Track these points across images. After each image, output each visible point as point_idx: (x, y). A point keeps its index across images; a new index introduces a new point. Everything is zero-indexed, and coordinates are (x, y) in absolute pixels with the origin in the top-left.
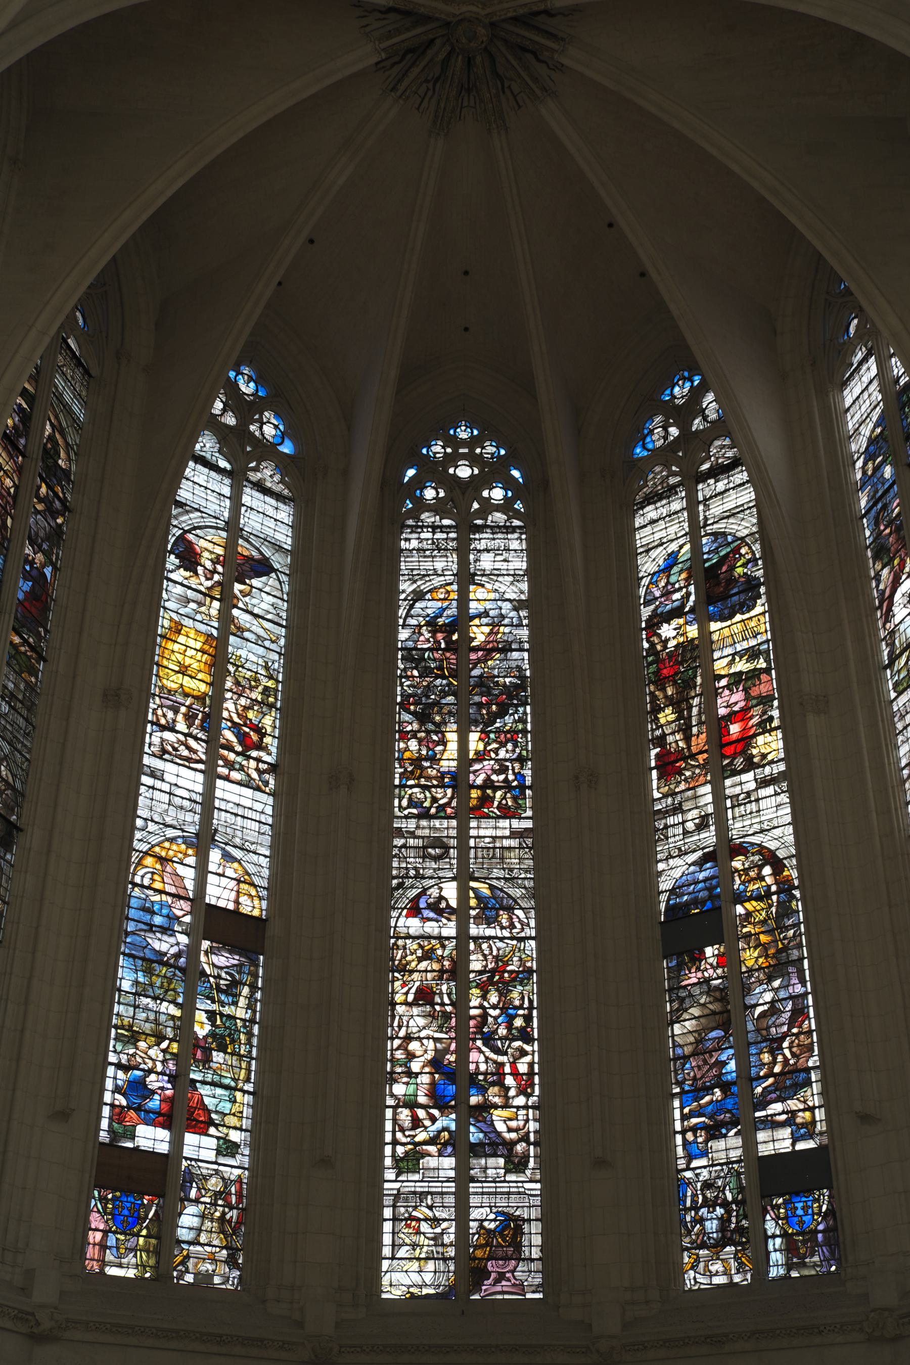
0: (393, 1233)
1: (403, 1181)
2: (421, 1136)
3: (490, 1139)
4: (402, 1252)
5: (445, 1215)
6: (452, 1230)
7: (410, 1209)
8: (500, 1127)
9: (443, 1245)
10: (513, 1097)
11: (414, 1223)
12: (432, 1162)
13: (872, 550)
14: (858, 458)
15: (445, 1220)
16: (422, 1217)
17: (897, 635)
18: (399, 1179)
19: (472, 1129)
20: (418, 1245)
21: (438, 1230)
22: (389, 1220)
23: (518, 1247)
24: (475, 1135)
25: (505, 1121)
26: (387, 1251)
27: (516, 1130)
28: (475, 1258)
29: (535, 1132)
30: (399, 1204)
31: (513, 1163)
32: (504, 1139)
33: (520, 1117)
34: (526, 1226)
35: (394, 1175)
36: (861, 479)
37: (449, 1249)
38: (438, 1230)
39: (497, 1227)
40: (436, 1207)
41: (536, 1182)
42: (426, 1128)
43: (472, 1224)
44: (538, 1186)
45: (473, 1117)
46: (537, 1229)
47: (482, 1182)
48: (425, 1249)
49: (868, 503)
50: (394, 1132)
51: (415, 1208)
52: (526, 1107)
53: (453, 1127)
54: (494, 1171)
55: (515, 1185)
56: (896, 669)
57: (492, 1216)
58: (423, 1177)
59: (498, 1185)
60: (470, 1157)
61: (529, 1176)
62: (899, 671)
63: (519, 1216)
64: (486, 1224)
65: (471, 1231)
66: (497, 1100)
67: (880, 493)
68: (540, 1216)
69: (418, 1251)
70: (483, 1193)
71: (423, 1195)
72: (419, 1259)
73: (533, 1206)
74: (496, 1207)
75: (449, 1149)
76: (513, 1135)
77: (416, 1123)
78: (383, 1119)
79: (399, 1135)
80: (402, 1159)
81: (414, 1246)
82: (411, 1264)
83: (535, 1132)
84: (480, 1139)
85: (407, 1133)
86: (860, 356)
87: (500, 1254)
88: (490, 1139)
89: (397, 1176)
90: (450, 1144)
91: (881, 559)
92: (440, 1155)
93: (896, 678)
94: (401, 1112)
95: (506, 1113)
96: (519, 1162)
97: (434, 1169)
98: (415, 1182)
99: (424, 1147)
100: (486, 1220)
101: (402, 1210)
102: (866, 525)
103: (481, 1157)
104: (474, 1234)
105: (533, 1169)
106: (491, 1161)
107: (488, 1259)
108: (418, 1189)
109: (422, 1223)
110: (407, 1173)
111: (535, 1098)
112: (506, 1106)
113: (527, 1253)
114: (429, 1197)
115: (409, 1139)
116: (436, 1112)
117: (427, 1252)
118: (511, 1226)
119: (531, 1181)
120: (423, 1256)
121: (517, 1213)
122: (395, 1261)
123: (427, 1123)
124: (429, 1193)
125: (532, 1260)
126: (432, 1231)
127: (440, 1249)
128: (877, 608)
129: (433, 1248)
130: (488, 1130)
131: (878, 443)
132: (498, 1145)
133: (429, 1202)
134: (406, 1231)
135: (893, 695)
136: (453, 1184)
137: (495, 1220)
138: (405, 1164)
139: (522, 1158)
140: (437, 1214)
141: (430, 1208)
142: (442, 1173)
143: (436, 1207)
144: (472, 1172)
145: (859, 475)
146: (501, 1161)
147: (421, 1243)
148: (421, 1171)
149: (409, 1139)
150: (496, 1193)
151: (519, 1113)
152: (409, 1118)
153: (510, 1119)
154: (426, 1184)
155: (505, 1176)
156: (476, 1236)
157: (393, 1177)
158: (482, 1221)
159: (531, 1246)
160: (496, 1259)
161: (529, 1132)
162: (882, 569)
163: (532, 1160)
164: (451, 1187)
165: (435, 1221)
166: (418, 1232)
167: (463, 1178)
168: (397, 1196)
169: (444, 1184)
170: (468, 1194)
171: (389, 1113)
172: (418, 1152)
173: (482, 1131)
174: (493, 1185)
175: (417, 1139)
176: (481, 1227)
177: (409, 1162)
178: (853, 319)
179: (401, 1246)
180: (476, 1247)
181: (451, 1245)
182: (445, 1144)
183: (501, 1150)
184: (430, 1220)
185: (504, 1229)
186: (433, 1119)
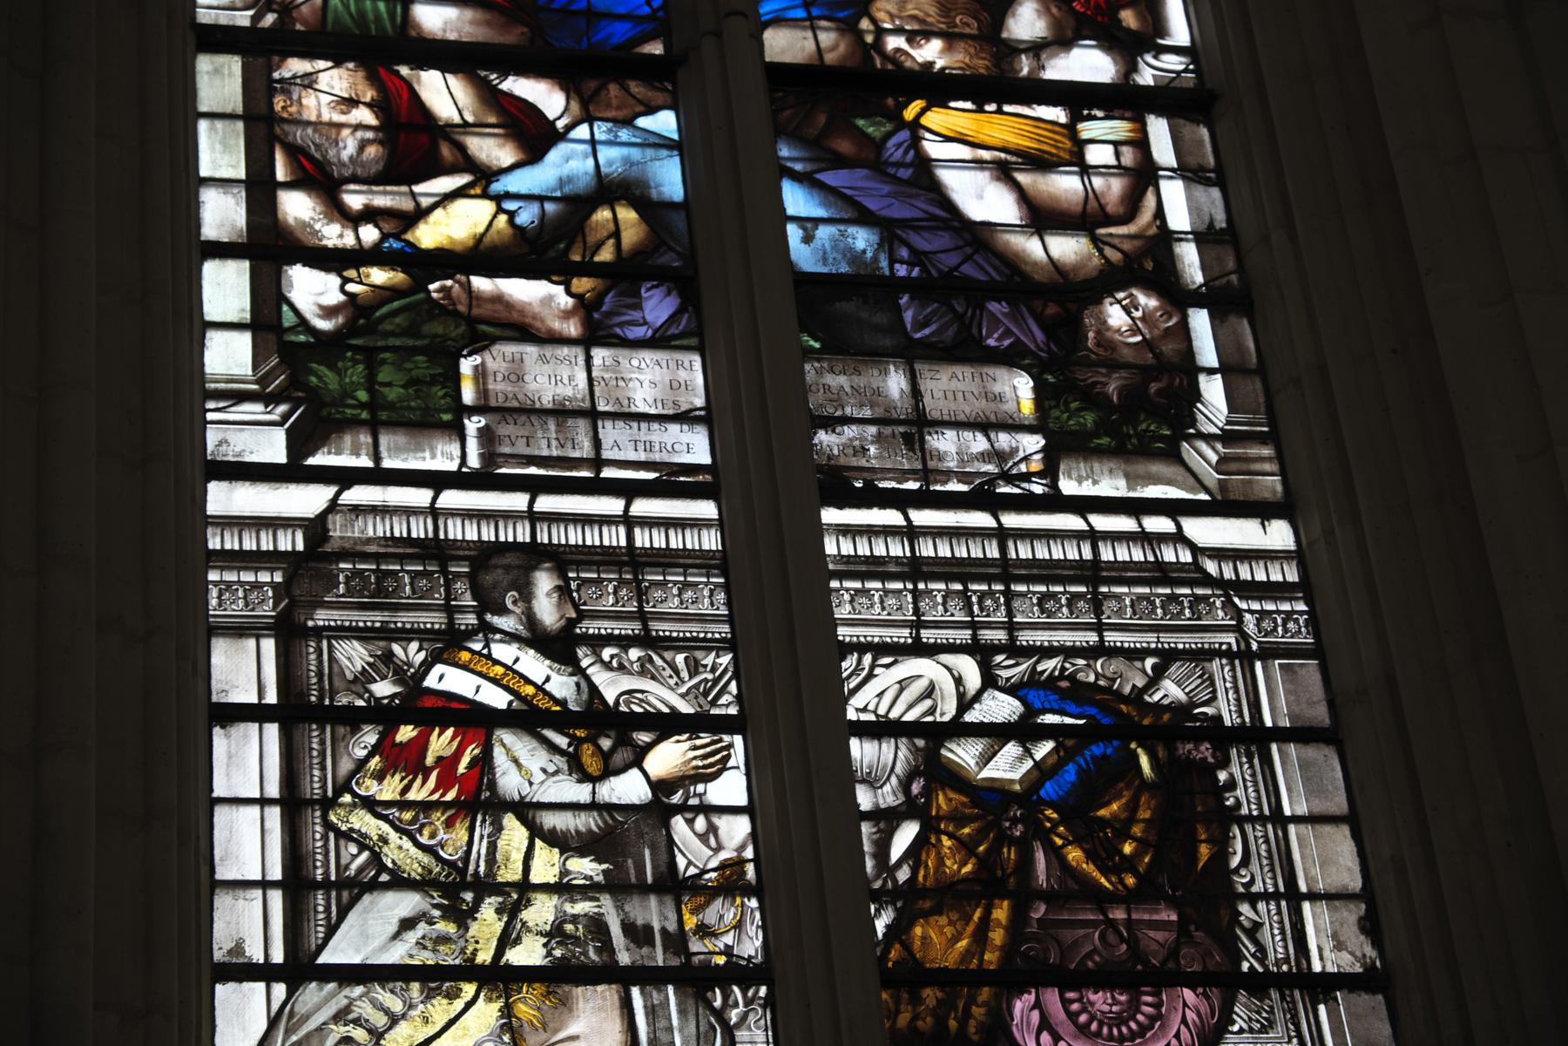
0: (293, 803)
1: (345, 478)
2: (457, 222)
3: (918, 257)
4: (369, 933)
5: (665, 696)
6: (730, 788)
7: (414, 653)
8: (984, 200)
9: (672, 885)
10: (1037, 49)
11: (441, 743)
12: (554, 377)
15: (667, 725)
16: (497, 698)
18: (319, 459)
19: (796, 200)
20: (486, 886)
21: (629, 788)
22: (255, 713)
23: (1211, 901)
24: (813, 230)
25: (1003, 172)
26: (247, 925)
27: (1086, 219)
28: (911, 976)
29: (1204, 237)
30: (322, 617)
31: (1092, 398)
32: (1013, 264)
33: (1099, 155)
34: (1237, 768)
35: (279, 437)
37: (721, 912)
38: (629, 788)
39: (1042, 771)
40: (596, 643)
41: (1262, 511)
42: (483, 179)
43: (862, 751)
44: (1279, 535)
45: (795, 137)
46: (1313, 787)
47: (901, 501)
48: (541, 911)
50: (259, 190)
51: (447, 645)
52: (1120, 99)
53: (669, 178)
54: (979, 443)
55: (1125, 523)
57: (1000, 708)
58: (489, 457)
59: (1011, 520)
60: (808, 354)
61: (1212, 477)
63: (1182, 711)
64: (964, 754)
65: (865, 799)
66: (931, 52)
68: (1320, 714)
69: (488, 922)
70: (916, 569)
71: (497, 570)
72: (499, 978)
73: (1268, 653)
74: (1015, 651)
75: (657, 307)
76: (1067, 248)
77: (414, 145)
78: (183, 116)
79: (297, 206)
80: (326, 346)
81: (457, 890)
82: (441, 1010)
83: (1204, 237)
84: (856, 258)
85: (355, 200)
87: (1088, 941)
88: (918, 257)
89: (300, 443)
90: (663, 277)
92: (598, 329)
94: (309, 81)
95: (1005, 127)
96: (1134, 401)
97: (561, 413)
98: (437, 481)
99: (481, 283)
100: (958, 729)
101: (353, 655)
103: (877, 356)
104: (887, 820)
105: (1227, 437)
106: (947, 386)
107: (1019, 974)
108: (455, 530)
109: (509, 741)
110: (375, 428)
111: (1173, 62)
112: (998, 81)
113: (1277, 946)
114: (544, 582)
115: (369, 234)
116: (547, 98)
117: (555, 933)
118: (1137, 783)
119: (1223, 506)
120: (529, 953)
121: (1171, 690)
122: (311, 993)
123: (494, 150)
124: (535, 554)
125: (1323, 987)
126: (580, 792)
127: (654, 913)
129: (606, 907)
130: (898, 211)
132: (978, 293)
133: (547, 610)
134: (389, 790)
136: (707, 509)
137: (1023, 731)
138: (356, 373)
139: (1147, 373)
140: (611, 687)
141: (558, 646)
142: (618, 441)
143: (596, 643)
144: (823, 437)
146: (1020, 389)
147: (510, 873)
148: (473, 425)
149: (369, 234)
150: (1005, 571)
151: (1088, 130)
152: (364, 115)
153: (1042, 163)
154: (518, 501)
155: (1050, 472)
156: (906, 835)
157: (272, 447)
158: (934, 734)
159: (1293, 897)
160: (1072, 980)
161: (1165, 238)
163: (1213, 391)
164: (696, 521)
165: (600, 734)
166: (480, 800)
167: (769, 478)
168: (314, 559)
169: (643, 507)
170: (819, 574)
171: (219, 81)
172: (443, 310)
173: (864, 217)
174: (982, 519)
175: (428, 235)
176: (933, 771)
177: (386, 361)
179: (353, 890)
180: (913, 902)
181: (730, 882)
182: (628, 275)
183: (1000, 323)
184: (562, 718)
185: (1094, 788)
186: (535, 136)
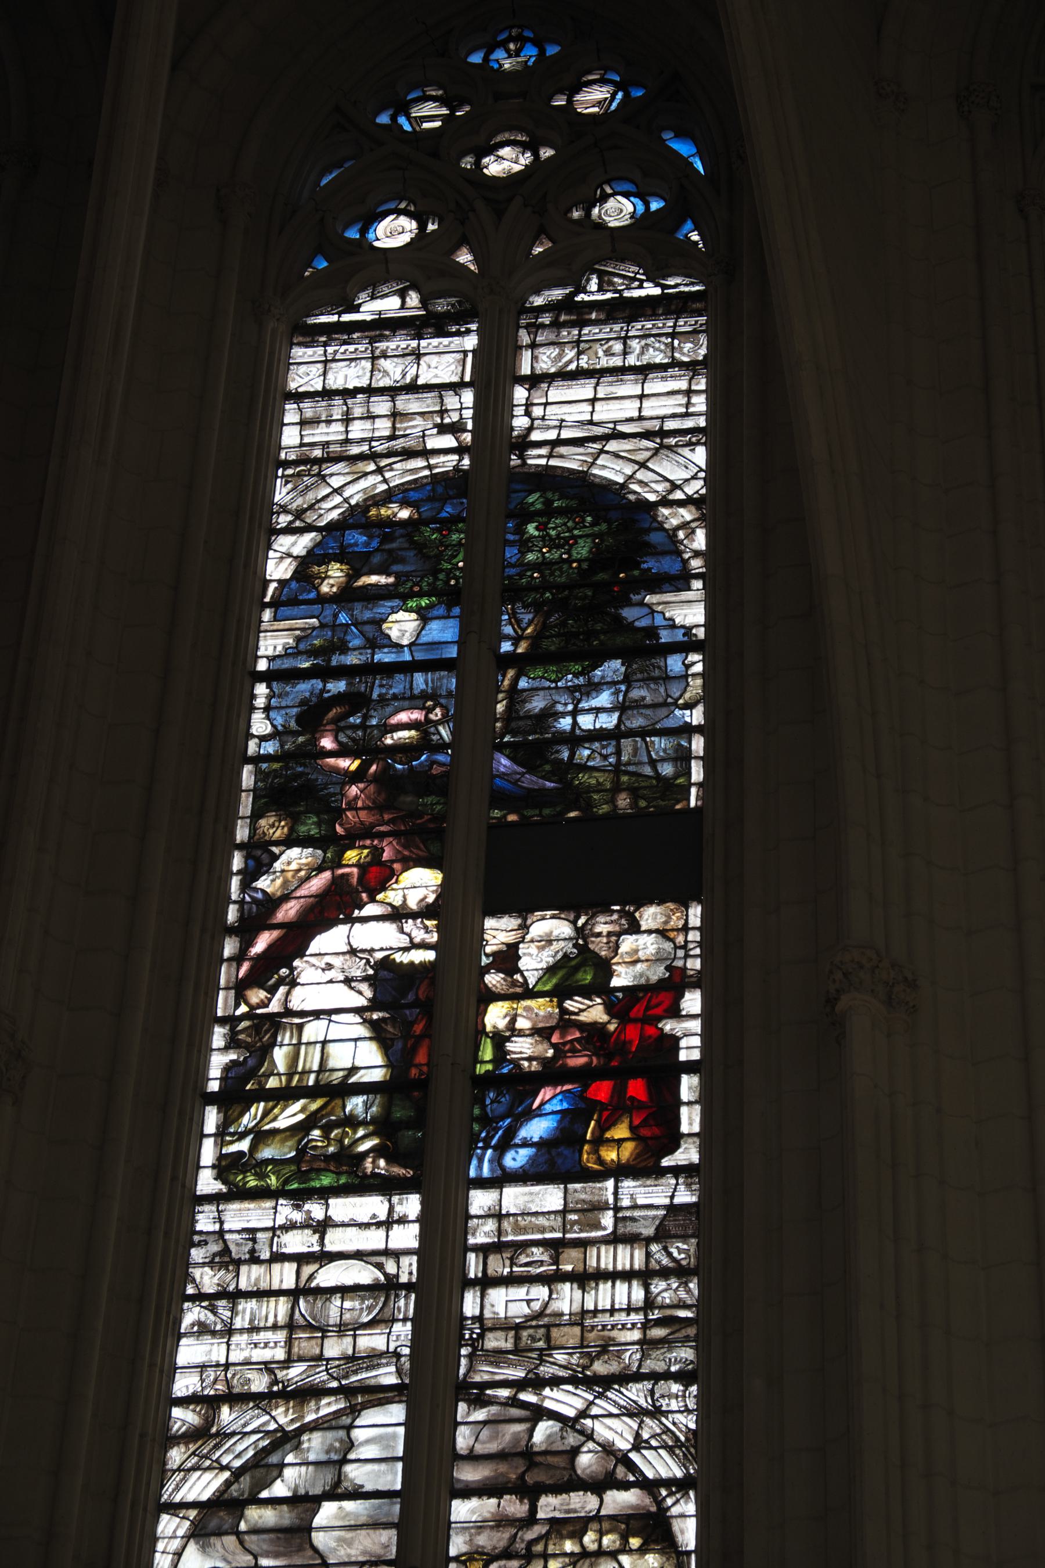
13: (258, 773)
14: (289, 530)
17: (286, 1037)
36: (282, 583)
49: (288, 653)
56: (247, 1121)
62: (260, 1136)
67: (352, 659)
86: (390, 305)
91: (295, 820)
93: (244, 1145)
102: (260, 702)
128: (231, 931)
131: (386, 539)
135: (207, 1183)
145: (278, 570)
162: (289, 843)
178: (399, 212)
